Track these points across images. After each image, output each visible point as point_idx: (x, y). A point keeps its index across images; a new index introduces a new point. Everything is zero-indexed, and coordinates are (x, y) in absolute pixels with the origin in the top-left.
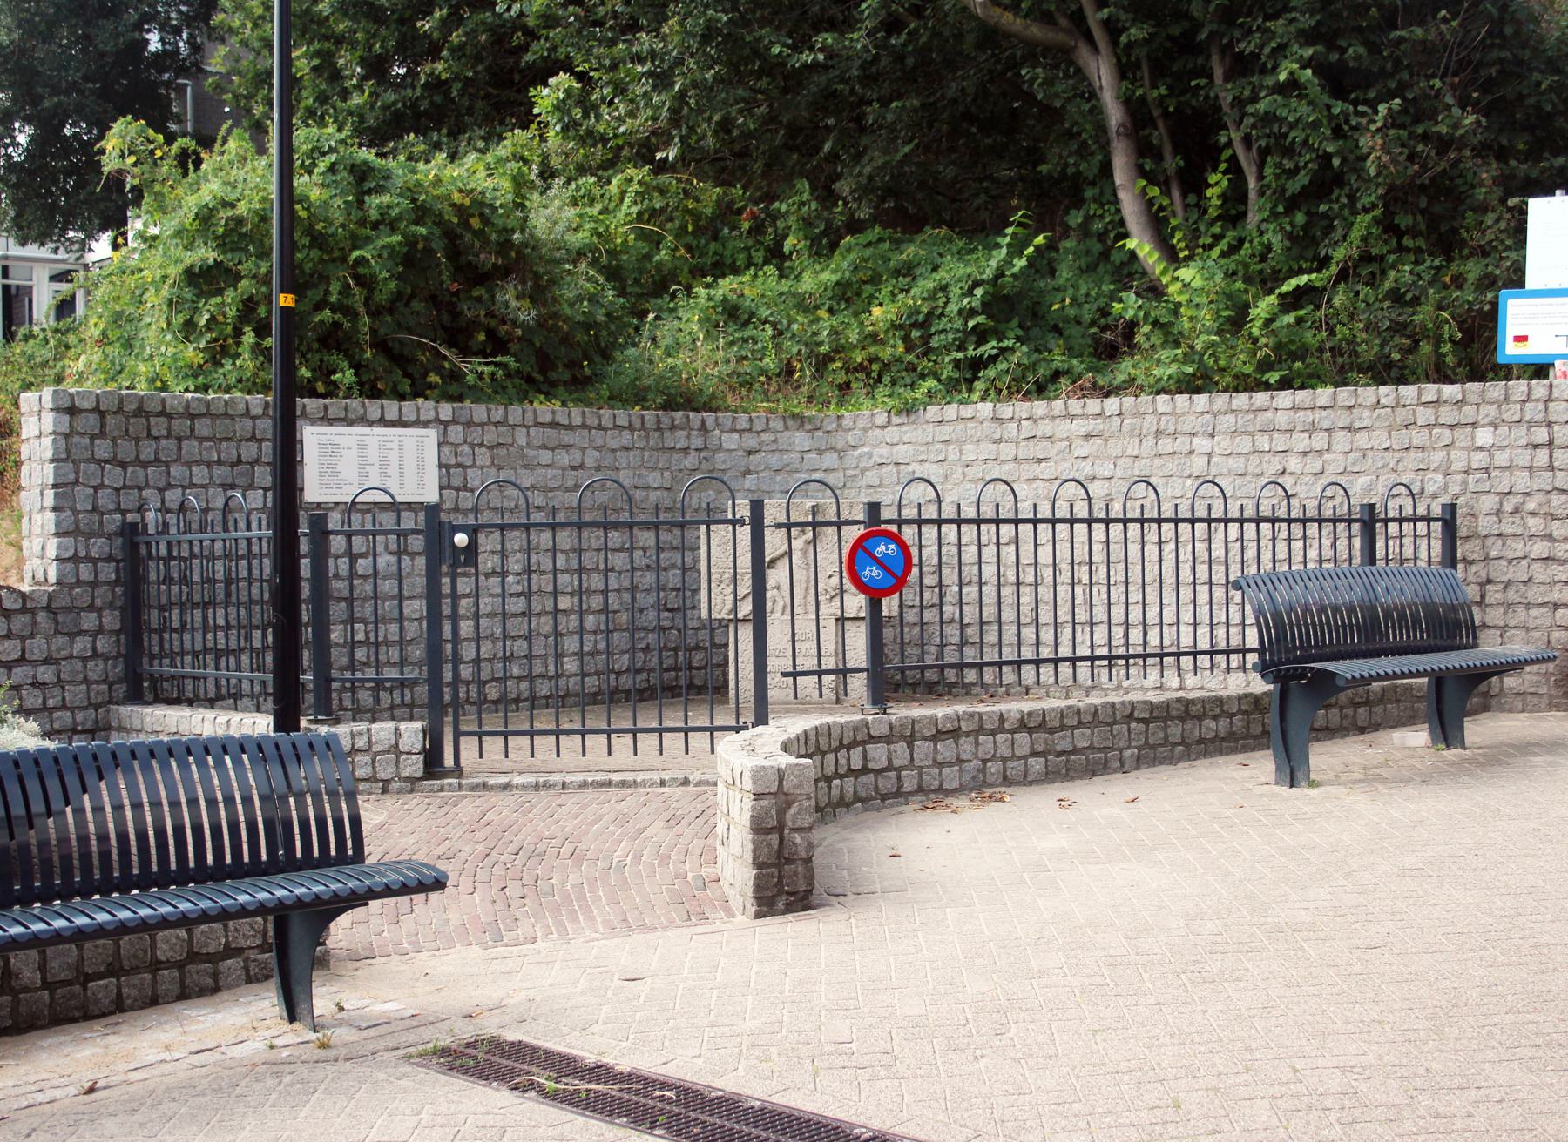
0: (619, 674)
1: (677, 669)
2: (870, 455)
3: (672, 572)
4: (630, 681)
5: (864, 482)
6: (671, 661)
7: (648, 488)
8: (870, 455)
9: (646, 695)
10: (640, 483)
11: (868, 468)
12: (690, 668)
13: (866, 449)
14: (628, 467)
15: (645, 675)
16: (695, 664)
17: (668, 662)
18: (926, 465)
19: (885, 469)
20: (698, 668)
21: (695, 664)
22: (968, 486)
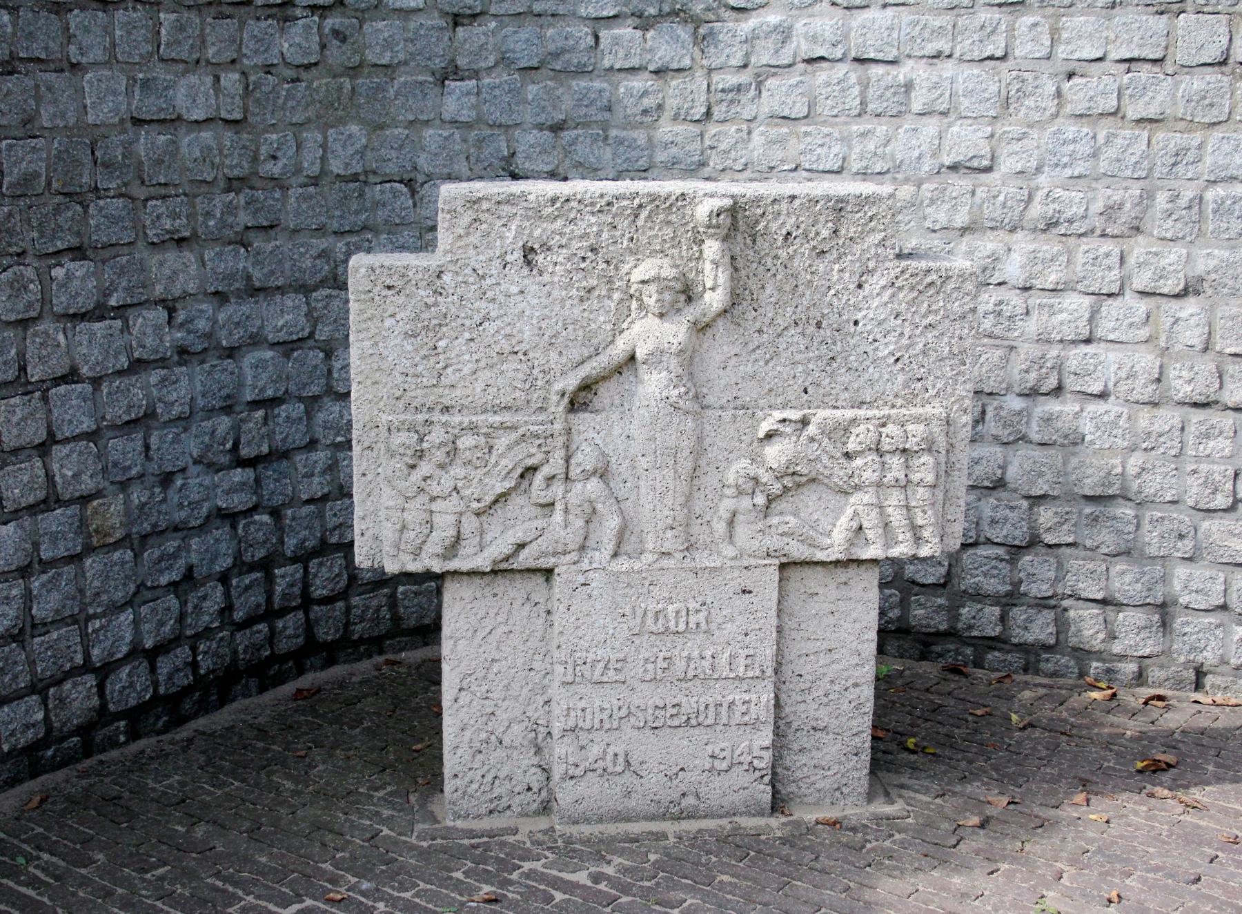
0: (105, 671)
1: (270, 614)
2: (784, 34)
3: (249, 359)
4: (142, 681)
5: (768, 103)
6: (256, 598)
7: (173, 122)
8: (784, 34)
9: (187, 705)
10: (149, 106)
11: (776, 69)
12: (307, 601)
13: (773, 18)
14: (111, 60)
15: (183, 653)
16: (318, 592)
17: (248, 601)
18: (948, 69)
19: (823, 74)
20: (327, 601)
21: (318, 592)
22: (1071, 130)
